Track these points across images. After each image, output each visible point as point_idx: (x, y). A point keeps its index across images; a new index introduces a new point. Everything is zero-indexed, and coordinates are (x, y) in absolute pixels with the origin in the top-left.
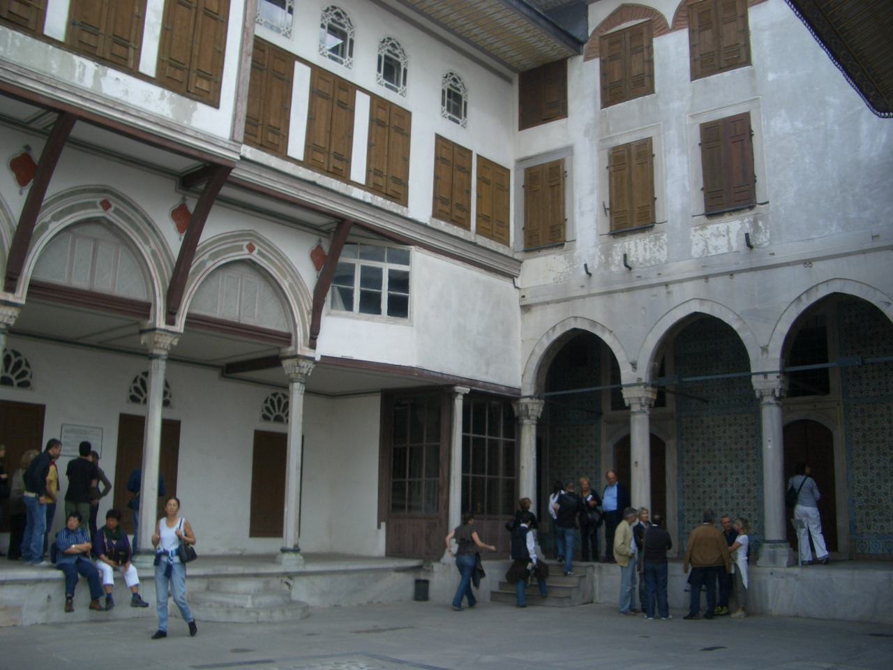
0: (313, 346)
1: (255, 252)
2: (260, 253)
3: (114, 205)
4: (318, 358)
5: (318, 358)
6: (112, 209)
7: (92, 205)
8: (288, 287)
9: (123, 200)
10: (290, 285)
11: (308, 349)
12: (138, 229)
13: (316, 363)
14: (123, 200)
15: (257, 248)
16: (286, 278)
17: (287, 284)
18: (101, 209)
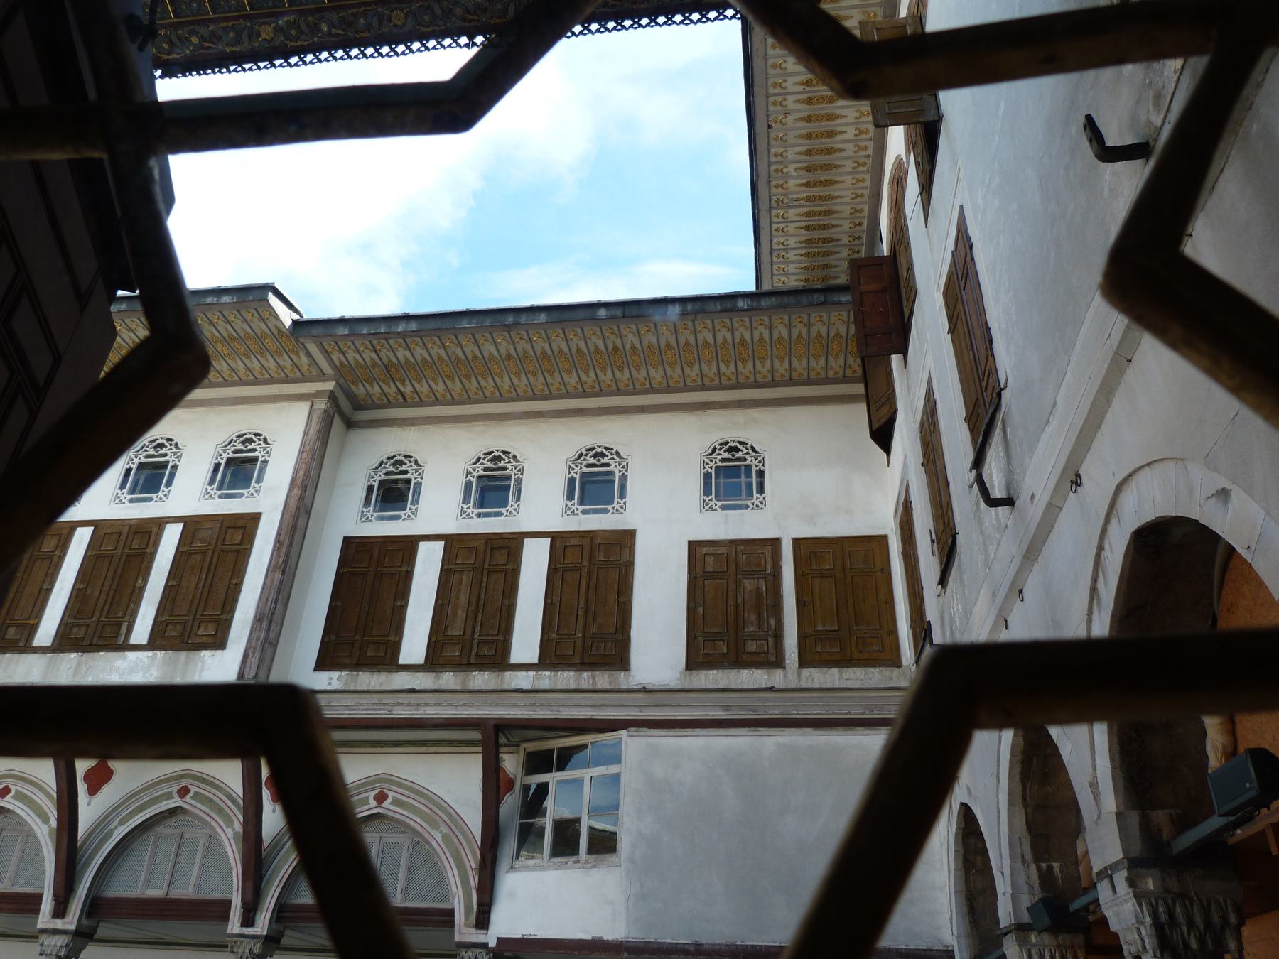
0: (483, 921)
1: (386, 804)
2: (396, 802)
3: (193, 789)
4: (492, 944)
5: (492, 944)
6: (191, 794)
7: (169, 796)
8: (439, 840)
9: (204, 781)
10: (445, 837)
11: (474, 930)
12: (220, 811)
13: (489, 950)
14: (204, 781)
15: (391, 795)
16: (437, 827)
17: (439, 837)
18: (177, 798)
